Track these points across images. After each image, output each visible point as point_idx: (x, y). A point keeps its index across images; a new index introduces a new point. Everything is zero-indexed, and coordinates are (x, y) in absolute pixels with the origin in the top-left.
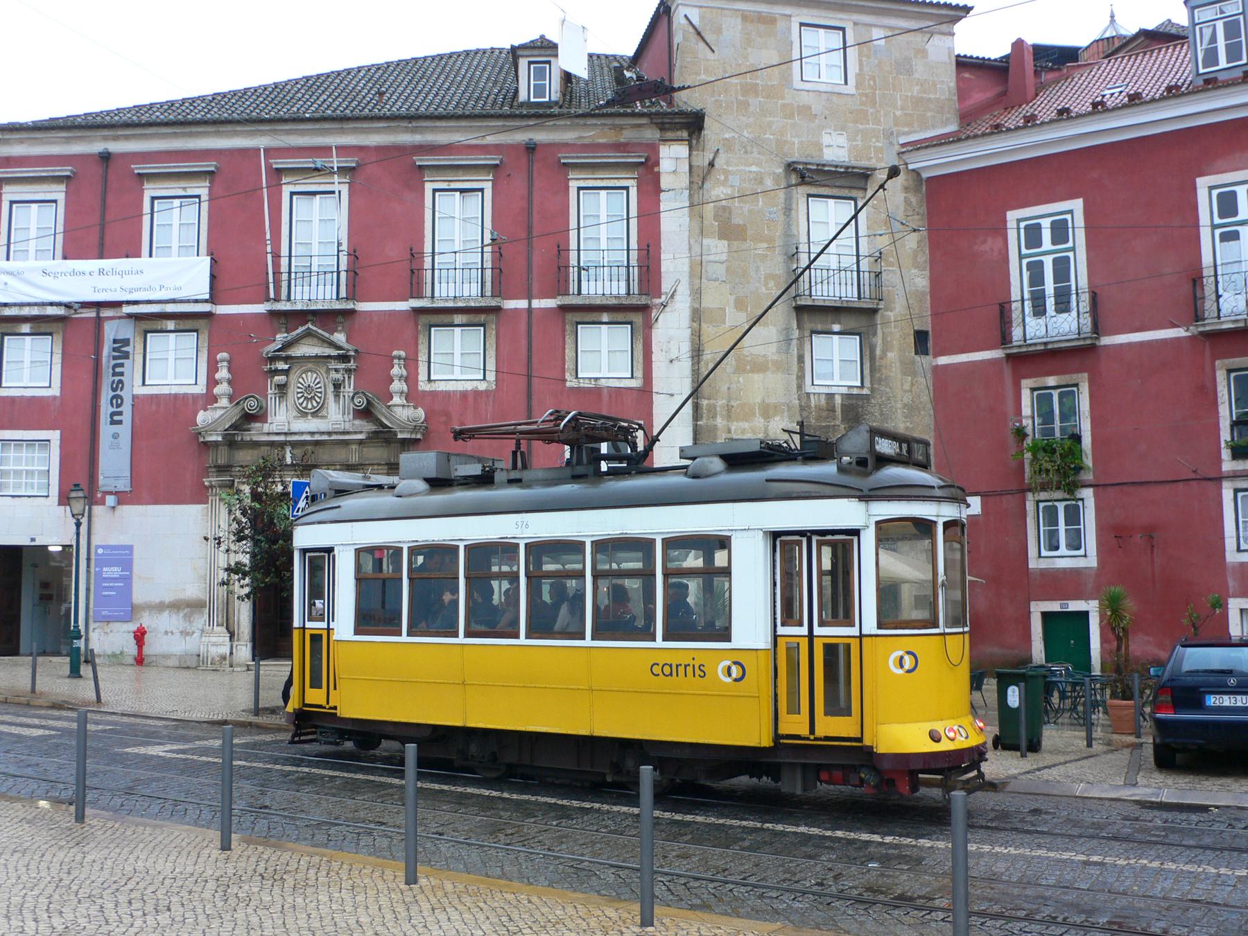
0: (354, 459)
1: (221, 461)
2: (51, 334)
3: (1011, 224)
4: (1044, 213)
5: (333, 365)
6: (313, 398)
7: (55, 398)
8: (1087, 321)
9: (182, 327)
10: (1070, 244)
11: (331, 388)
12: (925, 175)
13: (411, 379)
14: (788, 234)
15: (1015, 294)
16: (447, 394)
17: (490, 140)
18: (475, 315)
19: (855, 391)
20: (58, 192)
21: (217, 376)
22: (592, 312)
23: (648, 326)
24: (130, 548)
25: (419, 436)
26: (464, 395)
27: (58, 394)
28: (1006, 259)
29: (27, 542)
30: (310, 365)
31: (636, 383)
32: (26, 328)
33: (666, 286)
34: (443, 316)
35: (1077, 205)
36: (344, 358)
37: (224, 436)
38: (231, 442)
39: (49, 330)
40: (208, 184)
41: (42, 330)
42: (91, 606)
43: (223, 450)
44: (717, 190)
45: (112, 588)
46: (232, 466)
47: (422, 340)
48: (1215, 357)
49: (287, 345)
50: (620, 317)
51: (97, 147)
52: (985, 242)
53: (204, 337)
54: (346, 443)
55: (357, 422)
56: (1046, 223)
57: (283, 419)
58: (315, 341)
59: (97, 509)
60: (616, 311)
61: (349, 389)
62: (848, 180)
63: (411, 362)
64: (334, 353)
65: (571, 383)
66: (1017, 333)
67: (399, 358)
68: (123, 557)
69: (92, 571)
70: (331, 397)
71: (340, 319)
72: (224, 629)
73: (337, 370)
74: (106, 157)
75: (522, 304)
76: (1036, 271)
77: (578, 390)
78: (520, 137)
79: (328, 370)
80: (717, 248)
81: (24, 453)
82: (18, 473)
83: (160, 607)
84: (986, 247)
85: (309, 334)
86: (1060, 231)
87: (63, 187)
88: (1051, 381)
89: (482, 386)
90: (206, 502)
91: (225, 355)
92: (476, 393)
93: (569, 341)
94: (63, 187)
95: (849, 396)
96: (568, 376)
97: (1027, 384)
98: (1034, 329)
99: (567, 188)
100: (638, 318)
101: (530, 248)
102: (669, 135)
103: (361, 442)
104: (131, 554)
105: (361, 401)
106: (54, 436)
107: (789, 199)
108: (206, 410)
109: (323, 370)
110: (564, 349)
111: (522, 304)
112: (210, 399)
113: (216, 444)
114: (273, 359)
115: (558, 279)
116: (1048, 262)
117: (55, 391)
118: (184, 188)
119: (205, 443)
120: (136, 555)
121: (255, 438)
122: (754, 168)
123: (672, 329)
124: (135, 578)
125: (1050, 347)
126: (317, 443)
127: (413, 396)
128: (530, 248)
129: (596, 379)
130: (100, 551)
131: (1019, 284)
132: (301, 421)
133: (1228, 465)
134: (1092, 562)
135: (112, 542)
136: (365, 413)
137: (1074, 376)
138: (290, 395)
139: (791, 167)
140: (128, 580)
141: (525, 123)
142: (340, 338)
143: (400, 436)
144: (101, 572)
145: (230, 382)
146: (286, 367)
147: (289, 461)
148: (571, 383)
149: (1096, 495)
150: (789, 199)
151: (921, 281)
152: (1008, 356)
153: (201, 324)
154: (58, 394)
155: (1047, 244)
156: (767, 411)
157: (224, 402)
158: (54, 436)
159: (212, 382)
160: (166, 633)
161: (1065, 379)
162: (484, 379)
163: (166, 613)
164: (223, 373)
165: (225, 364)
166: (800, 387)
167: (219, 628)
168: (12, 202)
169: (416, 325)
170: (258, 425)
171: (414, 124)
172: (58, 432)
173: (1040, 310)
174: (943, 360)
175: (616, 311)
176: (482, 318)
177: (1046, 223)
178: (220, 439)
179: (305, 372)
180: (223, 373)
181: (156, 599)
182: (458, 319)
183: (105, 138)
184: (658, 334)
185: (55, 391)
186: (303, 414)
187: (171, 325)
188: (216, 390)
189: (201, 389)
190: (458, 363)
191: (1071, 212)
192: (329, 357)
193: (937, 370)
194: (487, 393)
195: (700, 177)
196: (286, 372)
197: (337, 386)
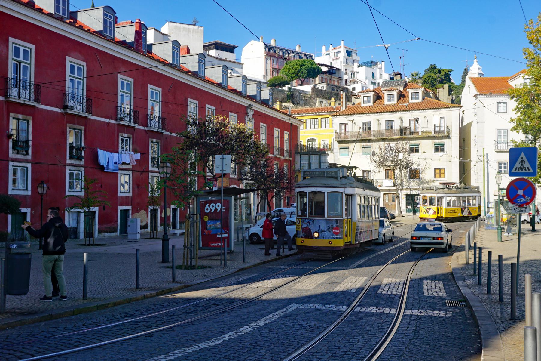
8: (33, 96)
10: (29, 62)
15: (9, 76)
35: (33, 47)
48: (67, 122)
76: (17, 68)
88: (20, 116)
97: (12, 115)
125: (26, 103)
133: (68, 161)
134: (29, 193)
137: (28, 117)
149: (32, 166)
152: (5, 101)
161: (25, 117)
177: (22, 49)
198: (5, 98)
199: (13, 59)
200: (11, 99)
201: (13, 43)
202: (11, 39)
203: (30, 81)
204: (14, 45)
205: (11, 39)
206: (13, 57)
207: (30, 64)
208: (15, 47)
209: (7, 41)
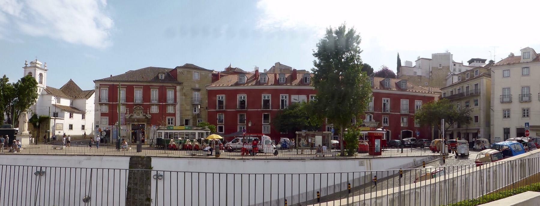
18: (156, 105)
20: (108, 89)
22: (169, 105)
23: (175, 107)
34: (153, 105)
44: (184, 91)
57: (135, 116)
60: (172, 105)
62: (198, 90)
78: (161, 85)
80: (184, 97)
101: (163, 97)
105: (144, 114)
115: (165, 101)
123: (178, 107)
127: (150, 113)
128: (163, 97)
136: (145, 116)
151: (207, 101)
156: (189, 115)
175: (172, 105)
190: (155, 110)
195: (182, 89)
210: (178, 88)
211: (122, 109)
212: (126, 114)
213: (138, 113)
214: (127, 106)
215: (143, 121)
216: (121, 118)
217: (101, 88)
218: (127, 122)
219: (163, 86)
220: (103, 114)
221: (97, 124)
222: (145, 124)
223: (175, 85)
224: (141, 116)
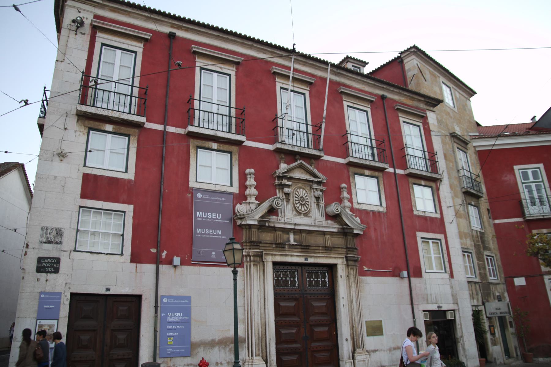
0: (329, 244)
1: (253, 239)
2: (128, 136)
3: (516, 172)
4: (529, 169)
5: (315, 186)
6: (304, 204)
7: (129, 181)
9: (221, 148)
10: (541, 180)
11: (314, 200)
12: (477, 149)
13: (351, 201)
14: (456, 162)
15: (522, 196)
16: (367, 212)
17: (367, 89)
19: (482, 231)
21: (248, 183)
23: (438, 189)
24: (189, 298)
25: (362, 233)
26: (374, 212)
27: (133, 178)
28: (516, 184)
29: (103, 292)
30: (300, 185)
31: (438, 216)
32: (109, 127)
33: (440, 171)
35: (541, 166)
36: (319, 183)
37: (259, 221)
38: (262, 226)
39: (128, 133)
40: (235, 69)
41: (122, 131)
42: (158, 345)
43: (254, 231)
45: (175, 330)
46: (260, 242)
47: (351, 180)
49: (289, 171)
50: (428, 183)
51: (166, 30)
52: (506, 176)
53: (236, 158)
54: (324, 233)
55: (329, 222)
56: (530, 172)
57: (288, 217)
58: (302, 171)
59: (163, 268)
61: (322, 203)
63: (350, 193)
64: (316, 180)
65: (415, 213)
66: (527, 213)
67: (345, 188)
68: (183, 305)
69: (159, 316)
70: (314, 206)
71: (313, 161)
72: (260, 358)
73: (316, 189)
74: (172, 36)
75: (391, 170)
77: (419, 217)
79: (311, 188)
81: (103, 218)
82: (94, 234)
83: (212, 344)
84: (506, 179)
85: (301, 167)
86: (535, 174)
87: (142, 45)
89: (381, 209)
90: (243, 267)
91: (252, 170)
92: (379, 213)
93: (411, 191)
94: (142, 45)
95: (480, 232)
96: (414, 209)
98: (533, 211)
99: (399, 121)
100: (433, 185)
102: (428, 108)
103: (332, 234)
104: (190, 303)
106: (129, 209)
107: (453, 147)
108: (241, 204)
109: (308, 189)
110: (410, 195)
111: (391, 170)
112: (241, 197)
113: (250, 225)
114: (279, 178)
116: (533, 186)
117: (131, 176)
118: (221, 68)
119: (241, 226)
120: (193, 305)
121: (277, 225)
122: (443, 131)
124: (193, 322)
125: (545, 217)
126: (309, 232)
129: (425, 212)
130: (165, 300)
131: (524, 195)
132: (298, 217)
135: (174, 294)
136: (336, 217)
138: (291, 201)
139: (451, 134)
140: (187, 323)
141: (382, 86)
142: (315, 171)
143: (355, 232)
144: (166, 316)
145: (256, 188)
146: (290, 183)
147: (292, 242)
148: (415, 213)
150: (453, 147)
153: (234, 149)
154: (133, 178)
155: (531, 179)
157: (253, 200)
158: (129, 209)
159: (243, 186)
160: (217, 364)
162: (381, 205)
163: (216, 349)
164: (251, 181)
165: (253, 176)
166: (470, 226)
167: (258, 358)
168: (103, 44)
169: (348, 172)
170: (275, 217)
171: (339, 71)
172: (132, 207)
173: (533, 203)
174: (497, 221)
176: (377, 174)
177: (530, 172)
178: (256, 223)
179: (300, 188)
180: (251, 181)
181: (208, 337)
182: (367, 172)
183: (173, 26)
184: (441, 193)
185: (131, 176)
186: (299, 213)
187: (215, 146)
188: (247, 192)
189: (235, 189)
191: (539, 168)
192: (312, 181)
193: (495, 224)
194: (383, 212)
196: (288, 186)
197: (318, 199)
198: (524, 218)
199: (523, 183)
200: (527, 218)
201: (519, 170)
202: (516, 168)
203: (547, 196)
204: (521, 171)
205: (516, 168)
206: (523, 181)
207: (542, 181)
208: (522, 172)
209: (513, 170)
210: (432, 117)
211: (212, 171)
212: (241, 197)
213: (302, 201)
214: (246, 158)
215: (328, 249)
216: (209, 226)
217: (101, 38)
218: (247, 241)
219: (383, 97)
220: (95, 187)
221: (49, 251)
222: (340, 262)
223: (422, 106)
224: (315, 220)
